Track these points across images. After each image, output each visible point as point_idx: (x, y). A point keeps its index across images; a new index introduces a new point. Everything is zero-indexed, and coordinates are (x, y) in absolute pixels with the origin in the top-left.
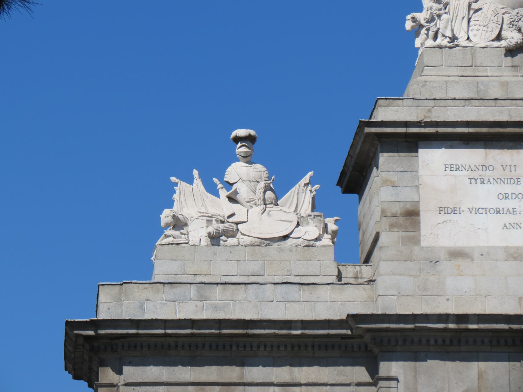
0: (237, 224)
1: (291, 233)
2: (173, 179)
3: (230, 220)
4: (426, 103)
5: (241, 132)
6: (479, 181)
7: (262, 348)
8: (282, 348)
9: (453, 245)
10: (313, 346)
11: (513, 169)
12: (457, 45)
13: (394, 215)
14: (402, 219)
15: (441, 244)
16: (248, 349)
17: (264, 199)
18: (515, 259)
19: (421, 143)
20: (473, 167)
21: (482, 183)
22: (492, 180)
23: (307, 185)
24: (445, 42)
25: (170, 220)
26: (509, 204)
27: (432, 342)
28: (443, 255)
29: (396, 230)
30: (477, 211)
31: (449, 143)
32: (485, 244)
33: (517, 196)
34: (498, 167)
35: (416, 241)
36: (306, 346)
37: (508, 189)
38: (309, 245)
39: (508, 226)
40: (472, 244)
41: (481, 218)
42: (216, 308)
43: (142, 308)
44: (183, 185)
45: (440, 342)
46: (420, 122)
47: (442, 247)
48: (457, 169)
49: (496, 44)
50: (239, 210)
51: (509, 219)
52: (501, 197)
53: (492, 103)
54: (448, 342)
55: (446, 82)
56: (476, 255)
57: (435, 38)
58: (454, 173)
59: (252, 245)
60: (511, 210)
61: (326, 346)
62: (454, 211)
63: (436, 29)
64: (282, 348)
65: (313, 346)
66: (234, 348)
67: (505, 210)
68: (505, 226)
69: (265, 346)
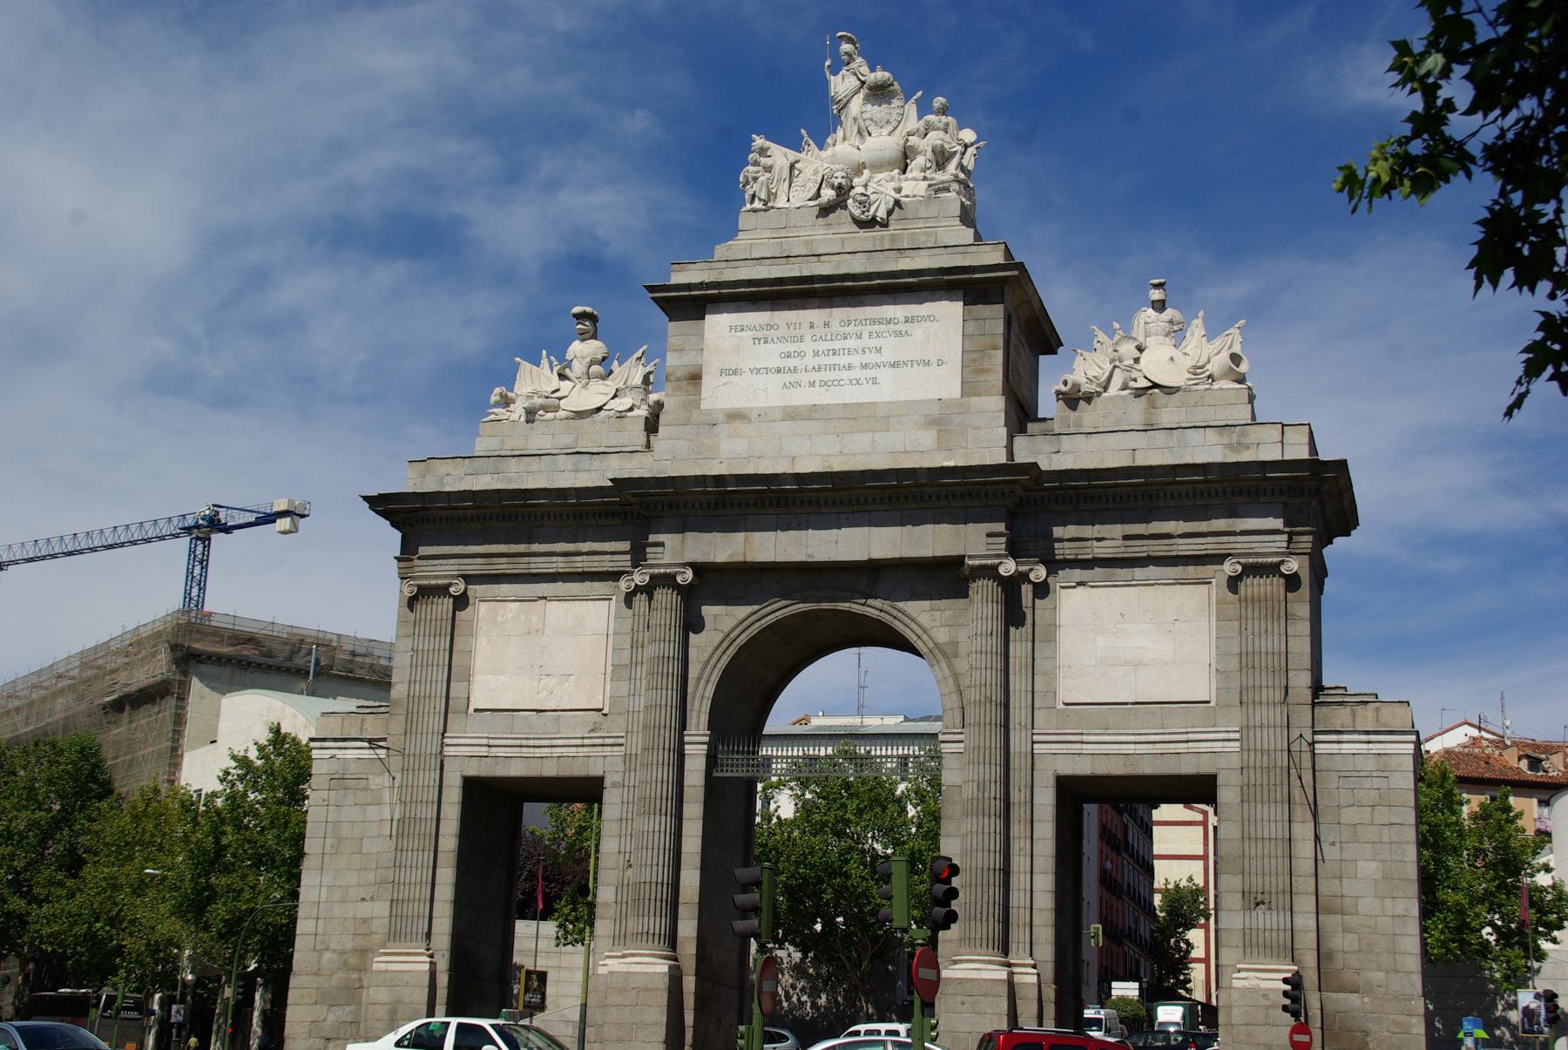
0: (560, 399)
1: (605, 405)
2: (518, 359)
3: (553, 395)
5: (577, 310)
6: (762, 341)
7: (545, 518)
8: (565, 517)
9: (731, 406)
11: (798, 327)
12: (772, 208)
13: (678, 380)
14: (685, 382)
15: (720, 407)
16: (533, 519)
17: (588, 374)
18: (792, 418)
19: (709, 306)
20: (758, 327)
21: (766, 342)
22: (775, 340)
23: (639, 359)
24: (757, 205)
25: (498, 398)
26: (791, 363)
27: (697, 506)
28: (721, 418)
31: (736, 303)
32: (763, 405)
33: (799, 354)
34: (783, 325)
36: (587, 514)
37: (791, 347)
38: (621, 415)
40: (748, 406)
42: (510, 480)
43: (441, 482)
44: (525, 366)
46: (701, 283)
47: (721, 410)
48: (742, 330)
49: (812, 203)
50: (566, 386)
51: (789, 378)
52: (783, 355)
54: (712, 506)
55: (751, 244)
56: (754, 416)
57: (752, 201)
58: (738, 334)
59: (567, 418)
62: (735, 372)
63: (752, 192)
64: (565, 517)
66: (520, 519)
68: (785, 385)
69: (549, 517)
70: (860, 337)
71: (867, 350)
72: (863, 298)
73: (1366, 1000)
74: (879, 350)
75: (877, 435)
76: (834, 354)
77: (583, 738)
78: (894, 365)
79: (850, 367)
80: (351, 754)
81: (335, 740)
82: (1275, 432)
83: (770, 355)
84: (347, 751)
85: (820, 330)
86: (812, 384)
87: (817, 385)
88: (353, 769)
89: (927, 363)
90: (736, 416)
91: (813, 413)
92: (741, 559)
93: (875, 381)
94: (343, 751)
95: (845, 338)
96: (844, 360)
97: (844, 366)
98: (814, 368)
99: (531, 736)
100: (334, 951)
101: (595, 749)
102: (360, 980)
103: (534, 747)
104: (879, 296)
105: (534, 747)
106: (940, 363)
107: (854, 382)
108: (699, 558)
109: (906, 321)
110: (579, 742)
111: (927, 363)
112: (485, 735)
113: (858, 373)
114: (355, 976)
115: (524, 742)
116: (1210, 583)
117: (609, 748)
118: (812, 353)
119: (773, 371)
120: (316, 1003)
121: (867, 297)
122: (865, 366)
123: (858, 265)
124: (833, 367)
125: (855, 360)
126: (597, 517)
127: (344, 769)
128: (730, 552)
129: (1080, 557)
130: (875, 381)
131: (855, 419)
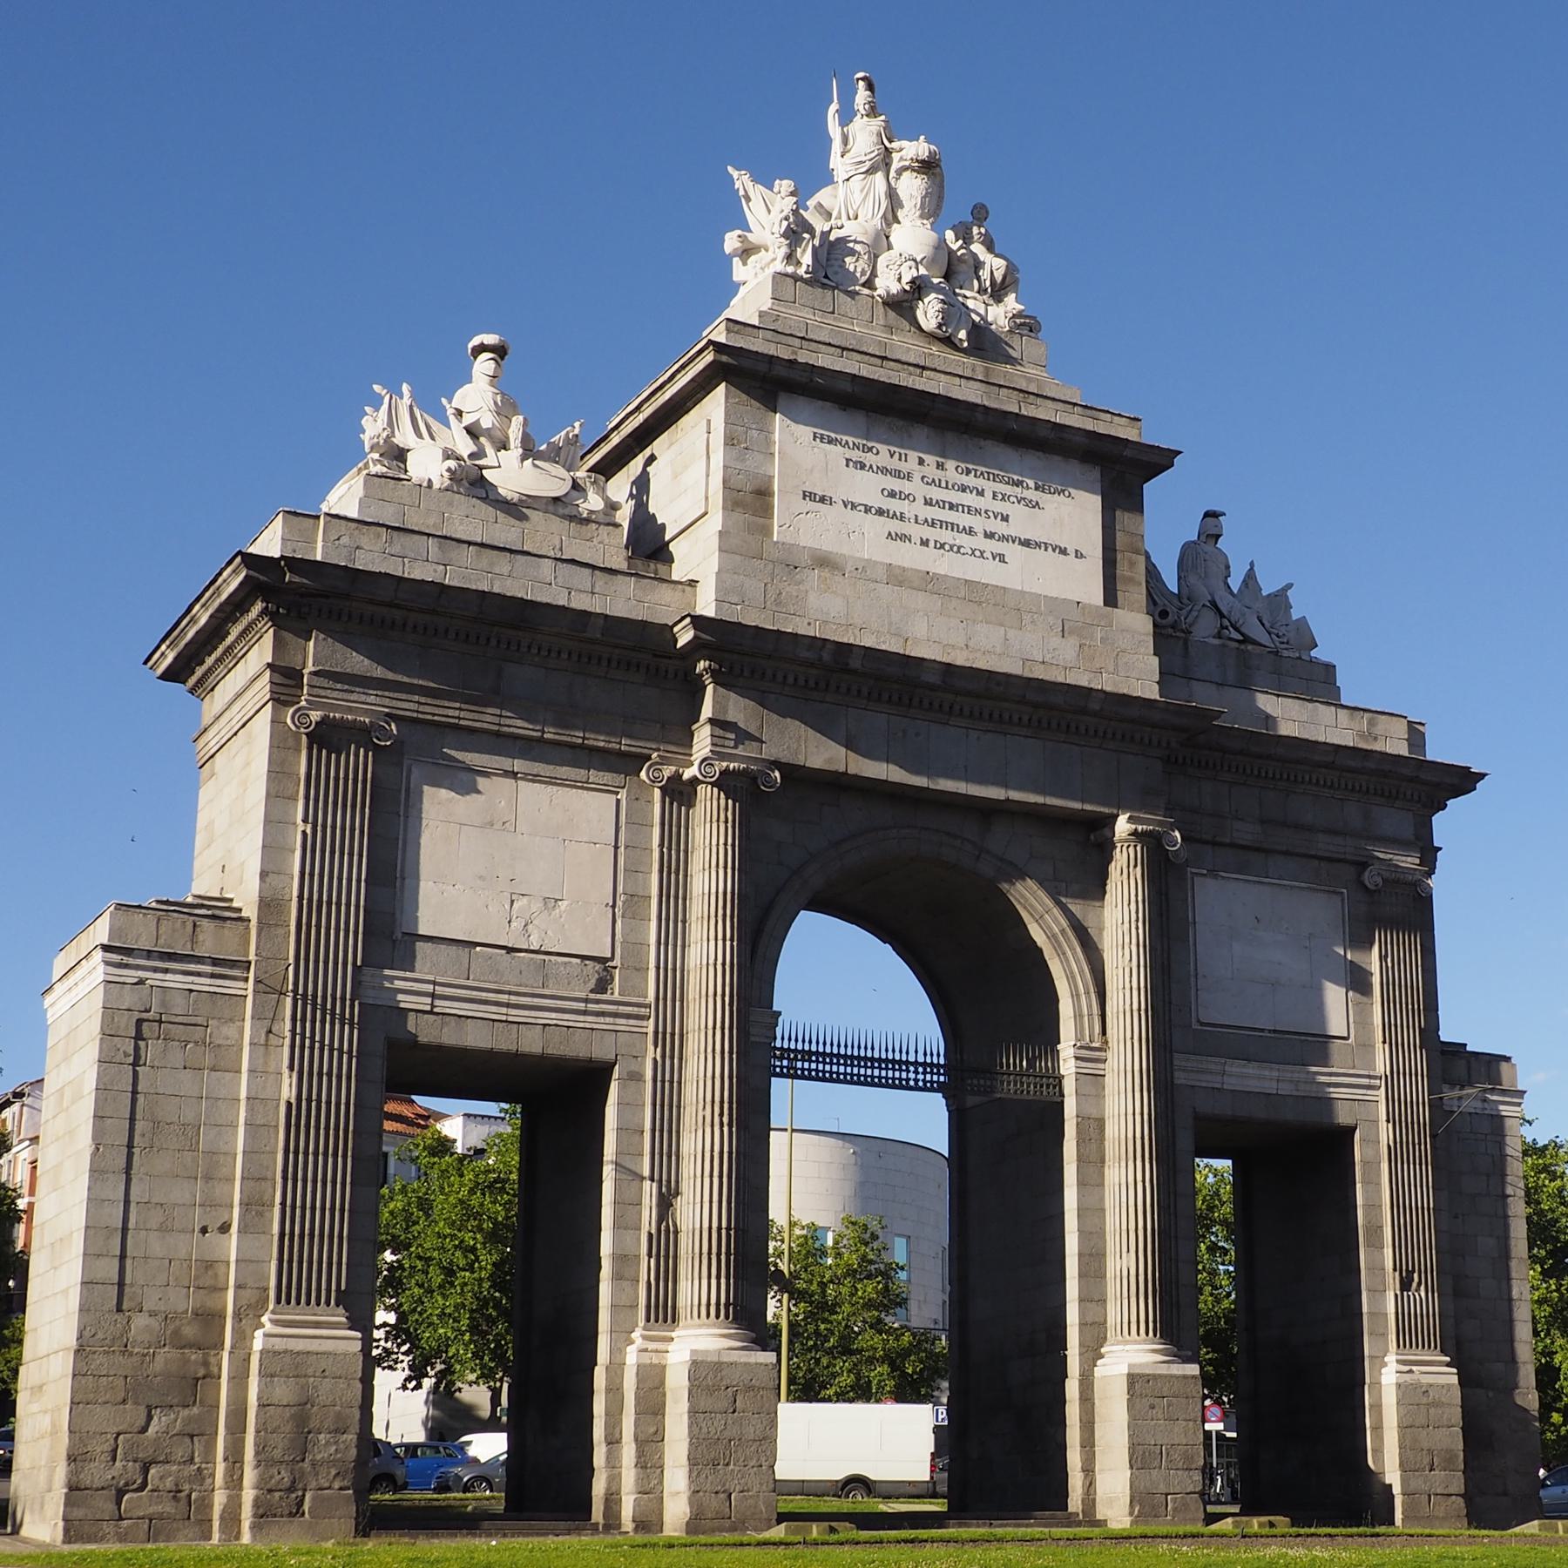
4: (790, 340)
8: (564, 656)
10: (609, 661)
19: (783, 399)
26: (894, 505)
27: (791, 680)
29: (740, 510)
30: (854, 506)
35: (767, 531)
36: (600, 659)
39: (894, 535)
40: (845, 551)
41: (859, 515)
45: (801, 682)
51: (895, 526)
53: (879, 362)
54: (812, 683)
56: (849, 567)
60: (898, 514)
61: (629, 664)
62: (822, 500)
64: (564, 656)
65: (609, 661)
67: (891, 513)
68: (890, 534)
70: (981, 493)
71: (991, 514)
72: (982, 443)
73: (1491, 1394)
74: (1005, 519)
75: (1011, 633)
76: (950, 509)
77: (586, 1001)
78: (1026, 543)
79: (971, 532)
80: (174, 981)
81: (149, 954)
82: (1401, 729)
83: (868, 487)
84: (169, 976)
85: (931, 471)
86: (925, 543)
87: (932, 544)
88: (179, 1006)
89: (1064, 552)
90: (824, 561)
91: (929, 582)
92: (842, 769)
93: (1002, 558)
94: (159, 976)
95: (964, 491)
96: (964, 520)
97: (964, 528)
98: (926, 521)
99: (507, 988)
100: (152, 1314)
101: (601, 1019)
102: (206, 1364)
103: (508, 1005)
104: (1002, 445)
105: (508, 1005)
106: (1079, 555)
107: (977, 553)
108: (785, 757)
109: (1036, 489)
110: (581, 1006)
111: (1064, 552)
112: (431, 978)
113: (980, 542)
114: (195, 1356)
115: (492, 997)
116: (1342, 893)
117: (623, 1021)
118: (923, 501)
119: (873, 511)
120: (124, 1401)
121: (989, 442)
122: (989, 535)
123: (971, 393)
124: (953, 526)
125: (978, 523)
126: (614, 664)
127: (163, 1003)
128: (827, 756)
129: (1218, 839)
130: (1002, 558)
131: (980, 603)
